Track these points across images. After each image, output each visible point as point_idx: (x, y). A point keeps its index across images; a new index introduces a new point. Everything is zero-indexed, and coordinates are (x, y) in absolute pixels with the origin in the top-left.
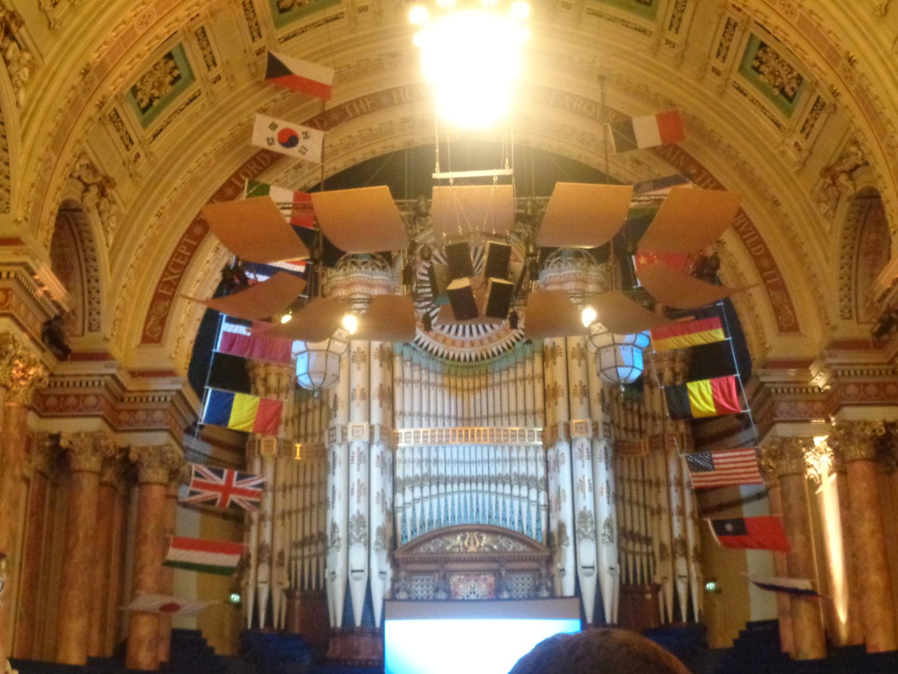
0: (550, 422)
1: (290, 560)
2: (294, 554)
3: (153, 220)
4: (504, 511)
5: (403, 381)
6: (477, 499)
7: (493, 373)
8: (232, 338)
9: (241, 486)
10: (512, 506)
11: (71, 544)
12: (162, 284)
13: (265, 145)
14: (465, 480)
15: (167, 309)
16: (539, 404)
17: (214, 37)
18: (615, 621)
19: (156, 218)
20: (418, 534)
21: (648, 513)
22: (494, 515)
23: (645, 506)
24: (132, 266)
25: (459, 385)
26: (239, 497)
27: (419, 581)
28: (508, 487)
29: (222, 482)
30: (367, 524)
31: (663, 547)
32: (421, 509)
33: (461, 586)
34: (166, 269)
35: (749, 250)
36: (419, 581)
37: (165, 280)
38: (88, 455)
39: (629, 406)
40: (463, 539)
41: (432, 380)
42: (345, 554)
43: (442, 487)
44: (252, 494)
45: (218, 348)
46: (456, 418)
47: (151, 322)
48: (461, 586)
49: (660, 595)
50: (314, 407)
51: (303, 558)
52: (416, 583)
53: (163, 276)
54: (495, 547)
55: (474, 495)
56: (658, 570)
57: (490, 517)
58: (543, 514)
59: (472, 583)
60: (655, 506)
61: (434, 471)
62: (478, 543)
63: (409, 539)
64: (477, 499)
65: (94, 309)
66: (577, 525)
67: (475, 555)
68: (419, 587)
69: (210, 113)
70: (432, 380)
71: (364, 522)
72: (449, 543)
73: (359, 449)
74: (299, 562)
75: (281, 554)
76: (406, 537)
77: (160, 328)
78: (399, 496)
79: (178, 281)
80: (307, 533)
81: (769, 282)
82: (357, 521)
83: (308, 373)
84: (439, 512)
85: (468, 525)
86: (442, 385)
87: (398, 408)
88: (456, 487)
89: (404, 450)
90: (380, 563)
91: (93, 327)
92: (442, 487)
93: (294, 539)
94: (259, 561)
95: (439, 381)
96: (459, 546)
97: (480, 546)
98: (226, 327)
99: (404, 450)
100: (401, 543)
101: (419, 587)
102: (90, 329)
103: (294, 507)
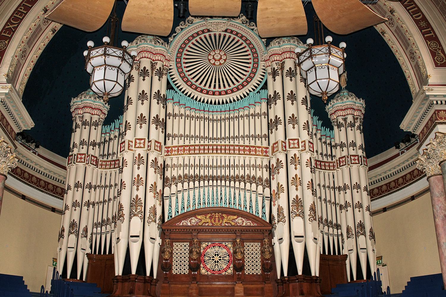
0: (272, 142)
1: (92, 234)
4: (240, 199)
10: (245, 197)
14: (213, 178)
16: (265, 131)
18: (317, 275)
21: (338, 208)
23: (335, 204)
28: (242, 184)
30: (143, 205)
32: (182, 199)
34: (9, 21)
35: (411, 16)
37: (7, 27)
39: (323, 140)
40: (211, 218)
42: (128, 225)
43: (197, 183)
49: (347, 262)
50: (115, 137)
51: (101, 233)
53: (6, 24)
56: (345, 245)
57: (229, 204)
58: (267, 203)
60: (343, 203)
62: (221, 221)
66: (291, 208)
74: (99, 237)
75: (86, 230)
78: (167, 189)
79: (16, 28)
81: (426, 36)
87: (169, 131)
92: (197, 183)
93: (95, 221)
94: (70, 233)
103: (97, 200)
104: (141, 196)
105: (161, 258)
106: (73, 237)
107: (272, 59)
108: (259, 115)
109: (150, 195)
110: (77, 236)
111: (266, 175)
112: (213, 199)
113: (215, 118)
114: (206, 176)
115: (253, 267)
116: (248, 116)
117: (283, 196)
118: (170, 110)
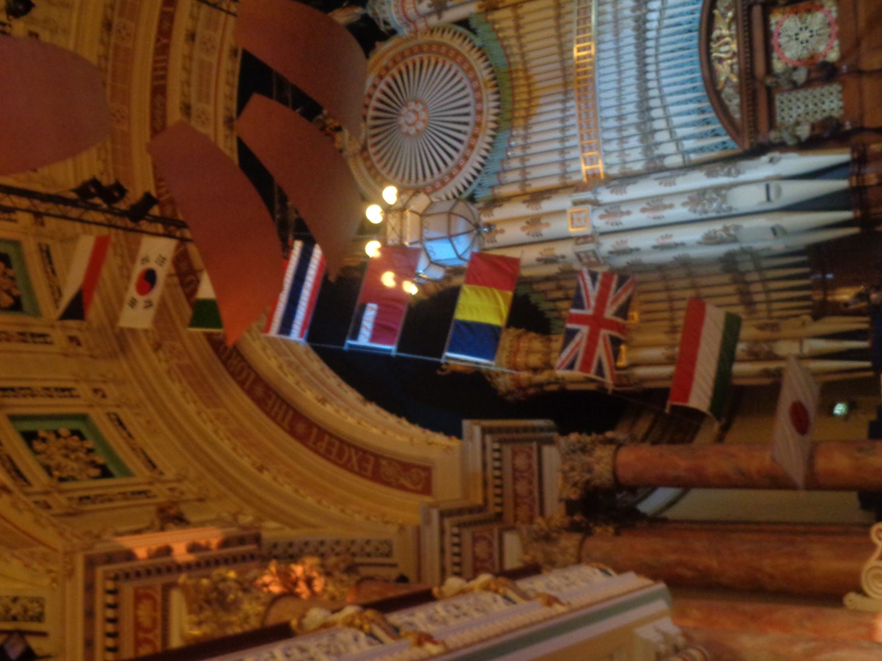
2: (763, 314)
3: (266, 476)
5: (524, 182)
6: (666, 52)
7: (510, 64)
8: (379, 332)
9: (593, 303)
11: (689, 574)
12: (361, 472)
13: (151, 312)
15: (391, 461)
17: (20, 379)
19: (266, 473)
20: (718, 126)
22: (686, 27)
24: (319, 502)
25: (524, 105)
26: (609, 304)
27: (783, 114)
29: (584, 329)
33: (788, 54)
36: (783, 114)
37: (356, 468)
38: (555, 550)
41: (520, 142)
44: (605, 286)
45: (391, 348)
46: (564, 101)
47: (408, 484)
48: (788, 54)
51: (769, 302)
52: (787, 119)
53: (351, 470)
54: (730, 14)
55: (661, 57)
57: (690, 31)
59: (782, 40)
61: (633, 119)
62: (728, 39)
63: (726, 138)
64: (666, 52)
65: (362, 549)
67: (741, 41)
68: (791, 112)
69: (151, 410)
70: (520, 142)
71: (698, 196)
72: (728, 79)
73: (602, 217)
74: (776, 306)
76: (724, 143)
77: (414, 470)
79: (358, 449)
80: (731, 289)
82: (698, 204)
83: (450, 237)
84: (686, 102)
85: (701, 61)
86: (526, 127)
87: (555, 182)
88: (653, 93)
89: (608, 166)
91: (386, 550)
95: (521, 132)
96: (731, 65)
97: (731, 36)
98: (364, 339)
99: (608, 166)
100: (734, 147)
101: (791, 112)
102: (388, 555)
107: (411, 12)
108: (517, 18)
110: (775, 340)
112: (682, 65)
113: (525, 96)
114: (637, 38)
116: (519, 37)
118: (514, 189)
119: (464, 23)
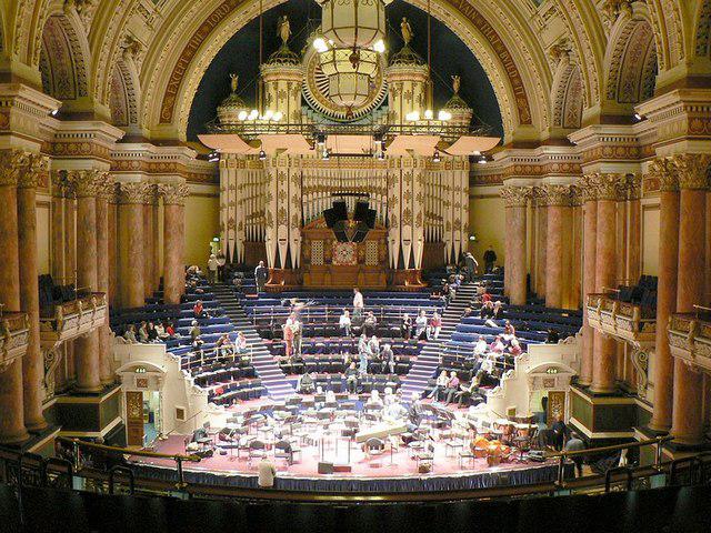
31: (448, 223)
90: (295, 234)
104: (286, 208)
105: (302, 255)
106: (231, 231)
109: (292, 206)
111: (384, 185)
115: (372, 260)
117: (397, 206)
119: (386, 103)
